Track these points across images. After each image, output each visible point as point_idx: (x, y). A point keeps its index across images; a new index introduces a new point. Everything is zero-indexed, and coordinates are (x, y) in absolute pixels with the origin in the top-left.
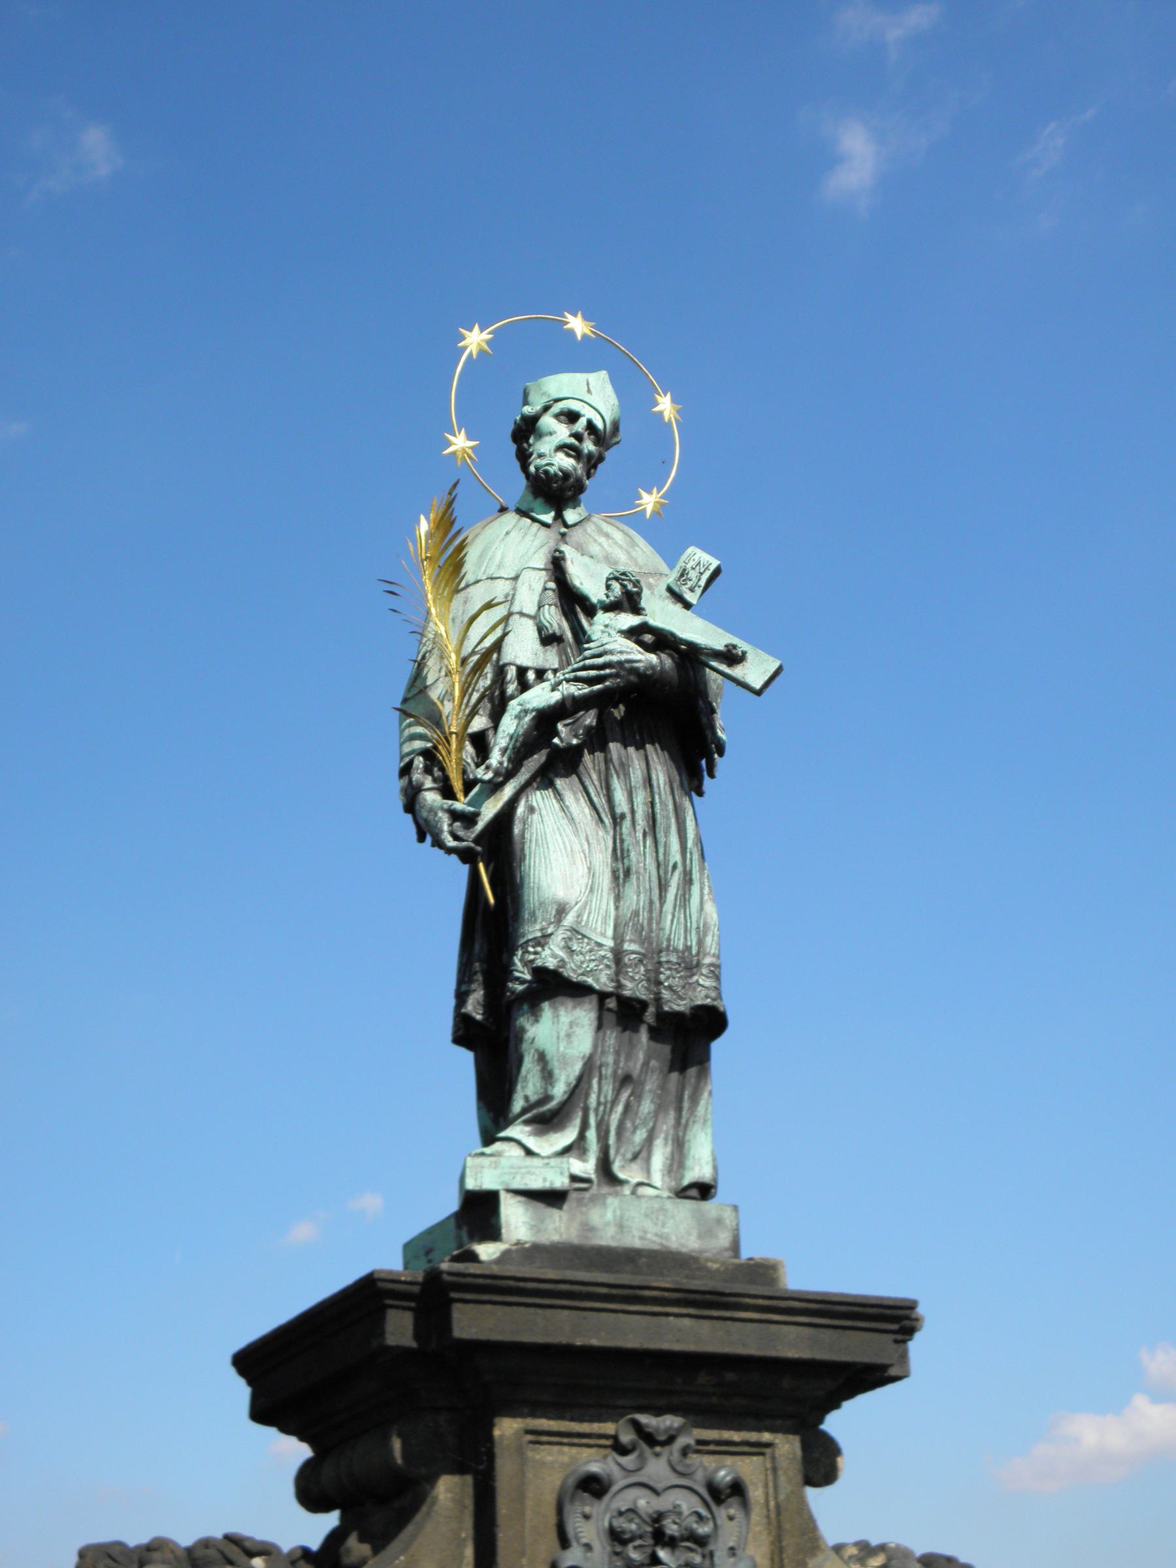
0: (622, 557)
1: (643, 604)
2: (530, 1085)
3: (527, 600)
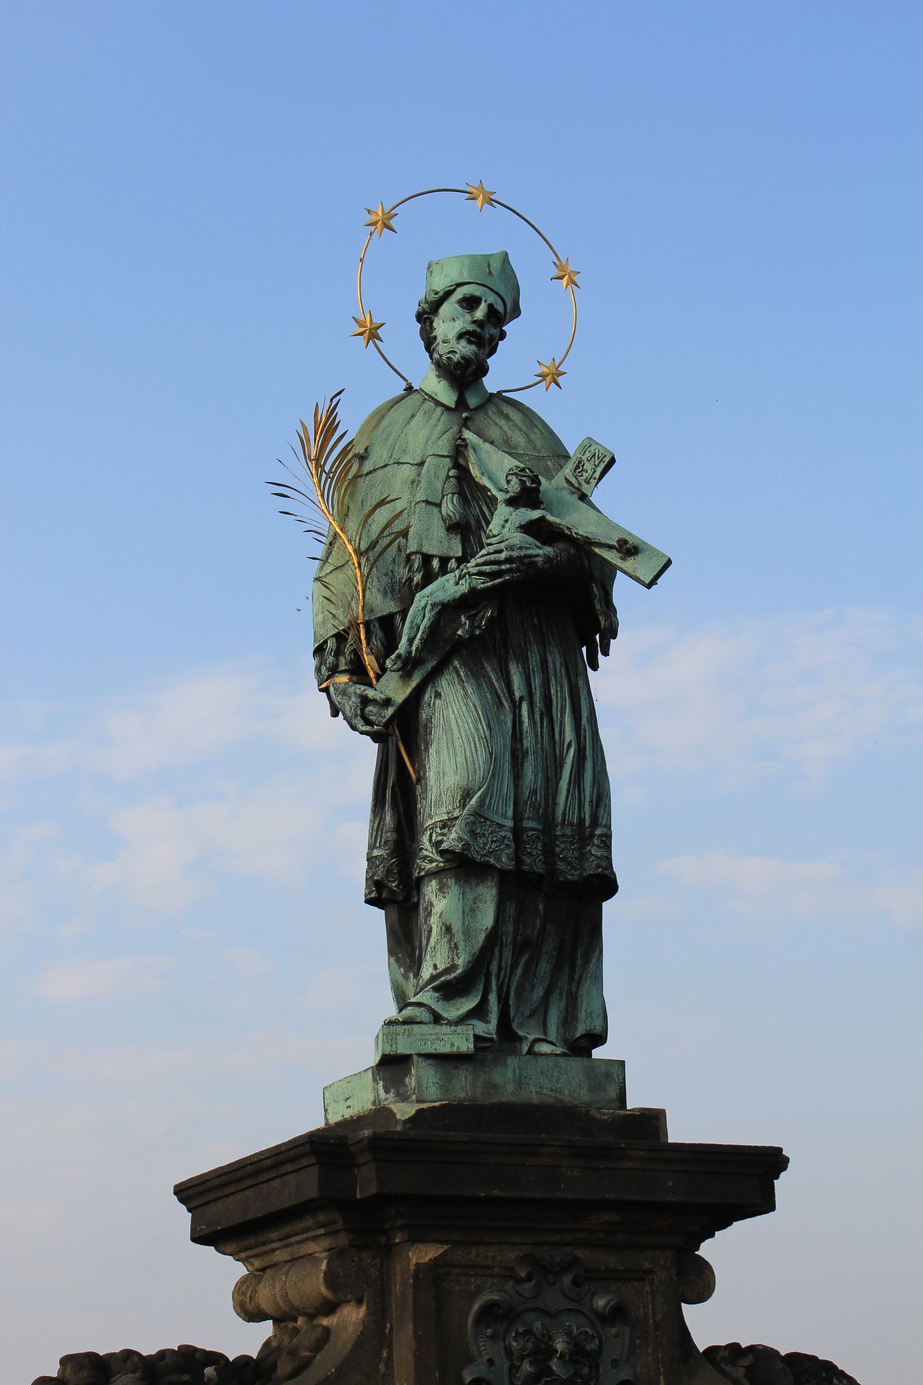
2: (438, 955)
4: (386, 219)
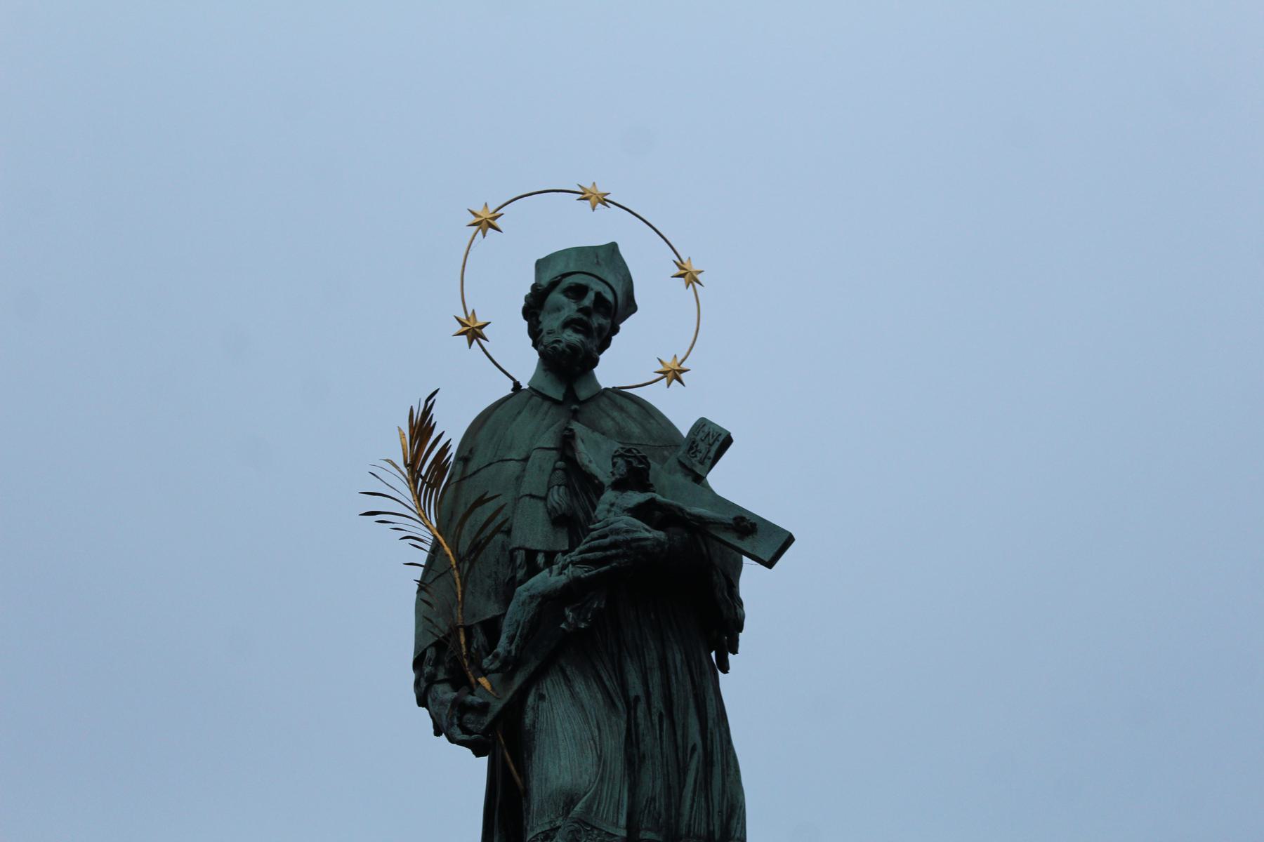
0: (635, 430)
1: (651, 480)
3: (535, 481)
4: (490, 218)
